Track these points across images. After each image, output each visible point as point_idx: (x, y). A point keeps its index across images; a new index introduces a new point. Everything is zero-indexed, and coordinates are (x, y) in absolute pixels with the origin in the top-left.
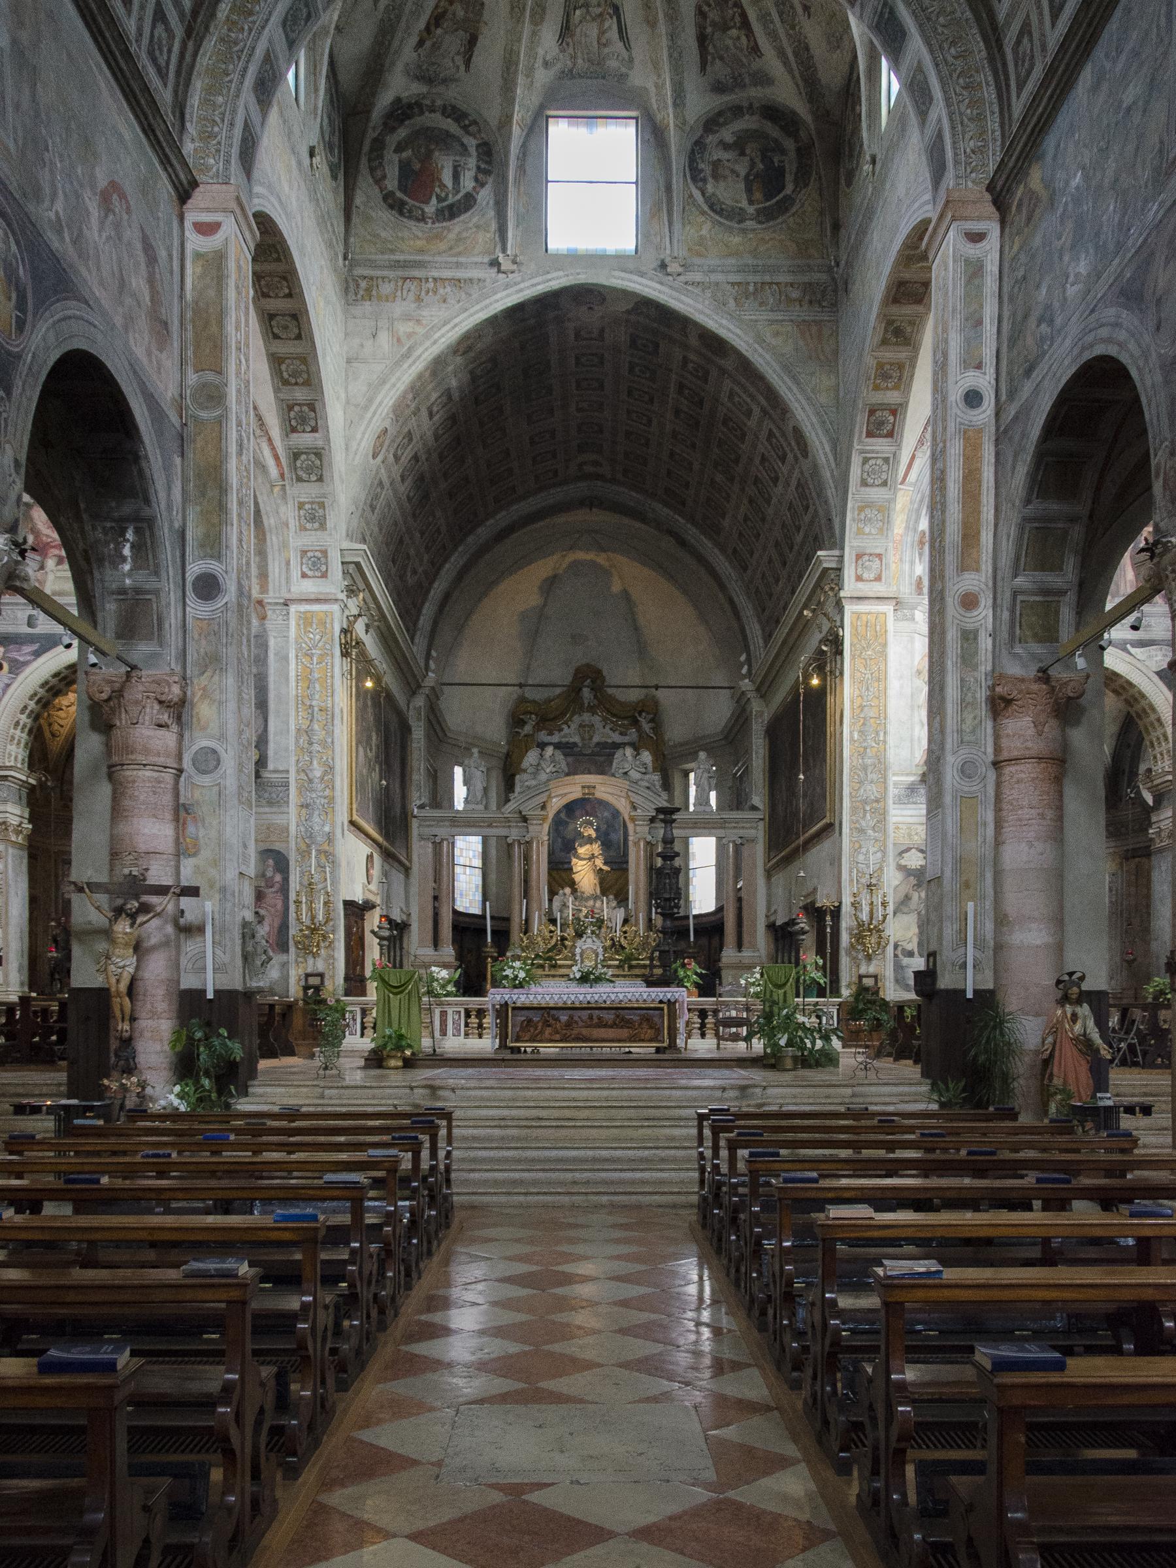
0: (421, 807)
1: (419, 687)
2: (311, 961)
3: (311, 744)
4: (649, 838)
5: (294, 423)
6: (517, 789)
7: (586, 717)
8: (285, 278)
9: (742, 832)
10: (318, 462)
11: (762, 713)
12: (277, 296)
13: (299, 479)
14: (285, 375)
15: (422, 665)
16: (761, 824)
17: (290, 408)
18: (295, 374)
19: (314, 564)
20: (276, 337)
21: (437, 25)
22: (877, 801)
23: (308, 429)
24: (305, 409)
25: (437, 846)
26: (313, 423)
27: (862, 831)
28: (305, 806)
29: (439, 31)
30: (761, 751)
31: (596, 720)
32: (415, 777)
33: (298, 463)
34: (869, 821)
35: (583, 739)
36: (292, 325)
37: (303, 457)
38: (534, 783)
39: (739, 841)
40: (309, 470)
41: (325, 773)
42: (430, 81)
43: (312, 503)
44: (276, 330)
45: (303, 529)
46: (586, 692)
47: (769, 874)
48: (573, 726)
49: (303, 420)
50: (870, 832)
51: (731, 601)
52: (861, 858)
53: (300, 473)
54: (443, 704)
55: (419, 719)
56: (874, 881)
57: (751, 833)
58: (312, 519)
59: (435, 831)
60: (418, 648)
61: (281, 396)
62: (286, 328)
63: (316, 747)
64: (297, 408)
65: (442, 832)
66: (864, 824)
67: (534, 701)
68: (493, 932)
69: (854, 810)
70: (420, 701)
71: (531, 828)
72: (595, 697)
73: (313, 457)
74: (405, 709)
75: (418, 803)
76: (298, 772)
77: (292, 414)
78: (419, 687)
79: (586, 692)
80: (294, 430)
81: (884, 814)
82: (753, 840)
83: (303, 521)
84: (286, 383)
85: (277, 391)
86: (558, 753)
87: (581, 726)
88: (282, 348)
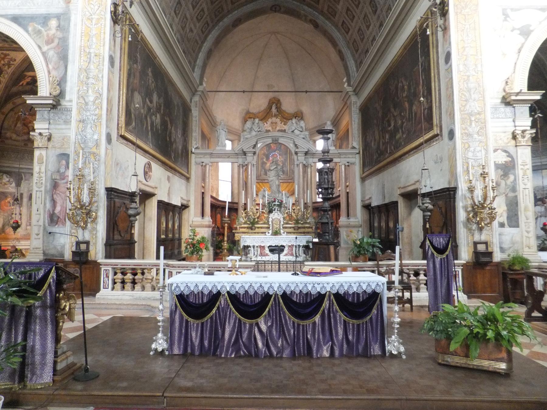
0: (197, 148)
1: (196, 91)
2: (80, 231)
3: (88, 78)
4: (305, 162)
6: (242, 140)
7: (274, 119)
9: (348, 160)
11: (356, 103)
15: (198, 82)
16: (357, 155)
22: (479, 114)
25: (204, 166)
27: (469, 135)
28: (82, 121)
30: (357, 121)
31: (278, 120)
32: (194, 134)
34: (474, 128)
35: (272, 128)
38: (249, 136)
39: (347, 164)
41: (96, 98)
46: (274, 110)
47: (363, 179)
48: (269, 123)
50: (476, 136)
51: (340, 53)
52: (470, 155)
54: (209, 102)
55: (196, 107)
56: (486, 171)
57: (351, 160)
59: (203, 160)
60: (196, 75)
63: (91, 81)
65: (206, 160)
66: (470, 130)
67: (253, 113)
68: (228, 208)
69: (463, 120)
70: (196, 98)
71: (248, 158)
72: (277, 111)
74: (189, 101)
75: (195, 146)
76: (78, 98)
78: (196, 91)
79: (274, 110)
81: (484, 126)
82: (353, 164)
86: (260, 122)
87: (272, 123)
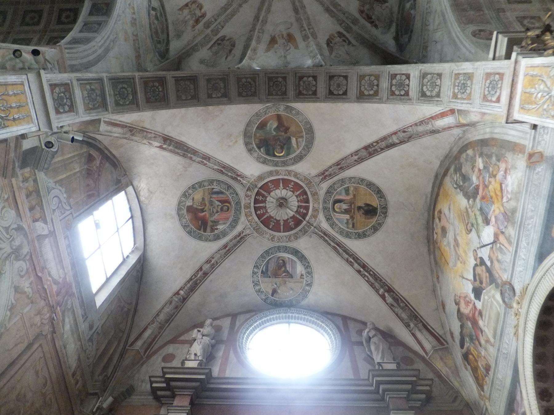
5: (403, 93)
8: (301, 78)
10: (429, 76)
12: (316, 86)
13: (438, 95)
14: (371, 92)
17: (393, 93)
18: (371, 85)
19: (493, 88)
20: (345, 93)
21: (371, 18)
23: (407, 82)
24: (394, 82)
26: (404, 77)
29: (373, 17)
33: (428, 93)
36: (336, 80)
37: (425, 89)
40: (434, 85)
42: (391, 22)
43: (455, 86)
44: (341, 92)
45: (469, 97)
49: (401, 85)
53: (434, 93)
58: (464, 86)
61: (385, 98)
62: (339, 85)
64: (394, 88)
73: (426, 80)
77: (397, 93)
80: (407, 94)
83: (464, 96)
84: (376, 93)
85: (381, 101)
88: (353, 91)
